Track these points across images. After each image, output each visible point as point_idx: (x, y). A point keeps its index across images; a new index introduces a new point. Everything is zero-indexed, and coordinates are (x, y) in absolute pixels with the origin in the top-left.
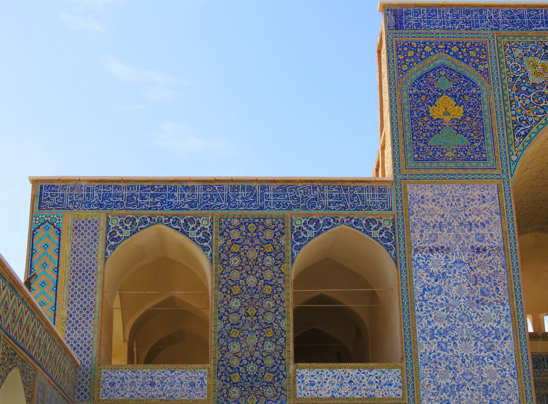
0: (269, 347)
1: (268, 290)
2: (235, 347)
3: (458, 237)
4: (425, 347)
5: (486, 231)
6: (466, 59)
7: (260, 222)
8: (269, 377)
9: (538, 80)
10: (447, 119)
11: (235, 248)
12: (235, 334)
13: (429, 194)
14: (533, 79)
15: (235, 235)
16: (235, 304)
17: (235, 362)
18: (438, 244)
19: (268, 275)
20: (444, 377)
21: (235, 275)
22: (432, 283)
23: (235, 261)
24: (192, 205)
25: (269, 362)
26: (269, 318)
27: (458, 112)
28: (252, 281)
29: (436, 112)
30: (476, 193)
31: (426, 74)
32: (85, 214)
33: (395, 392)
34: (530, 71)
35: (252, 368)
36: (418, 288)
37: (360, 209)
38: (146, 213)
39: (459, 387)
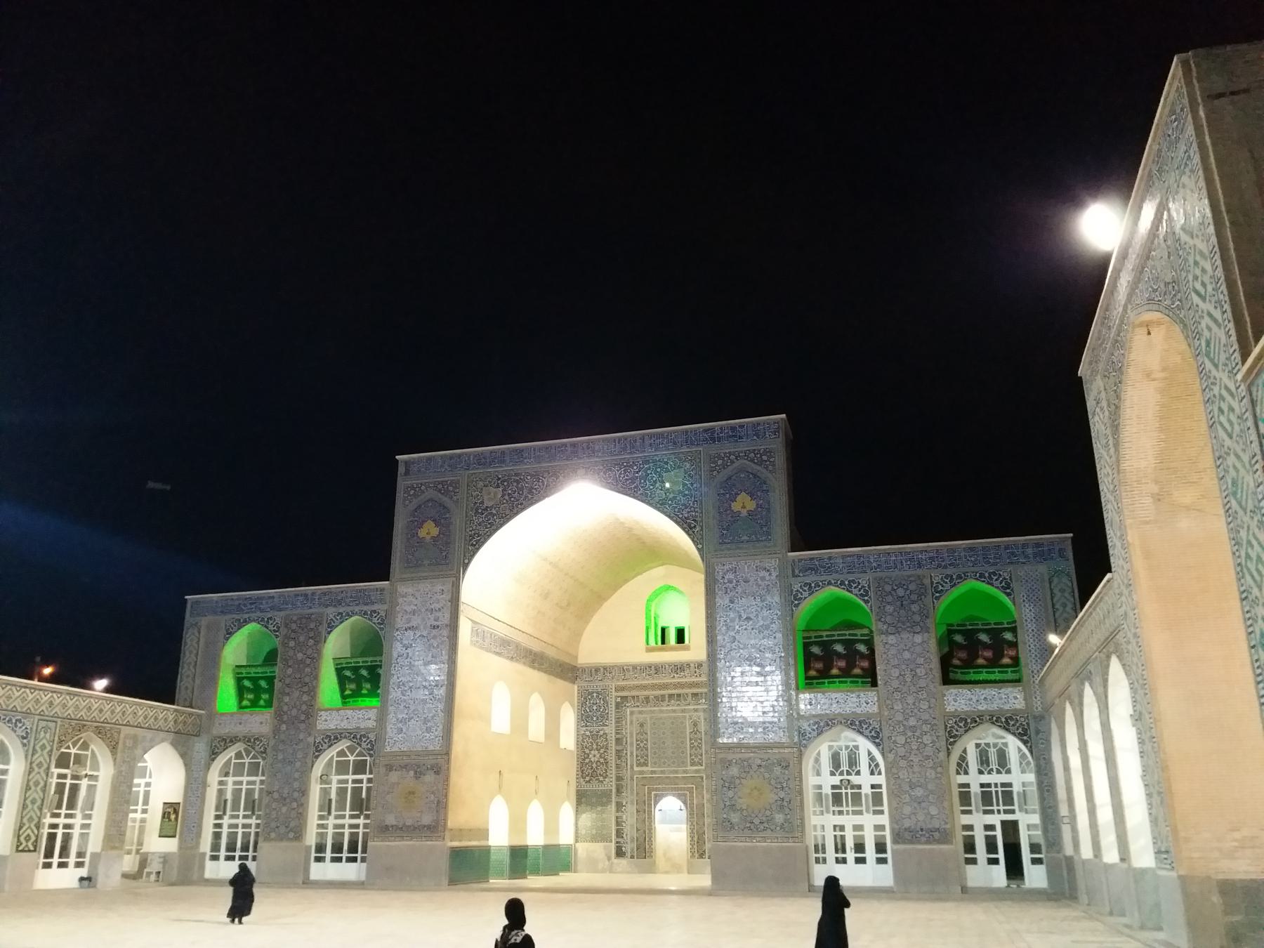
0: (305, 698)
1: (308, 661)
2: (287, 699)
3: (423, 619)
4: (394, 694)
5: (440, 614)
6: (446, 493)
7: (309, 618)
8: (303, 717)
9: (490, 504)
10: (428, 537)
11: (293, 635)
12: (287, 690)
13: (410, 590)
14: (488, 503)
15: (294, 626)
16: (290, 671)
17: (285, 708)
18: (410, 625)
19: (309, 652)
20: (402, 712)
21: (291, 653)
22: (404, 651)
23: (292, 644)
24: (272, 608)
25: (304, 707)
26: (307, 680)
27: (435, 531)
28: (300, 656)
29: (422, 533)
30: (439, 588)
31: (420, 506)
32: (210, 618)
33: (371, 724)
34: (486, 497)
35: (294, 712)
36: (395, 655)
37: (366, 604)
38: (246, 616)
39: (410, 719)
